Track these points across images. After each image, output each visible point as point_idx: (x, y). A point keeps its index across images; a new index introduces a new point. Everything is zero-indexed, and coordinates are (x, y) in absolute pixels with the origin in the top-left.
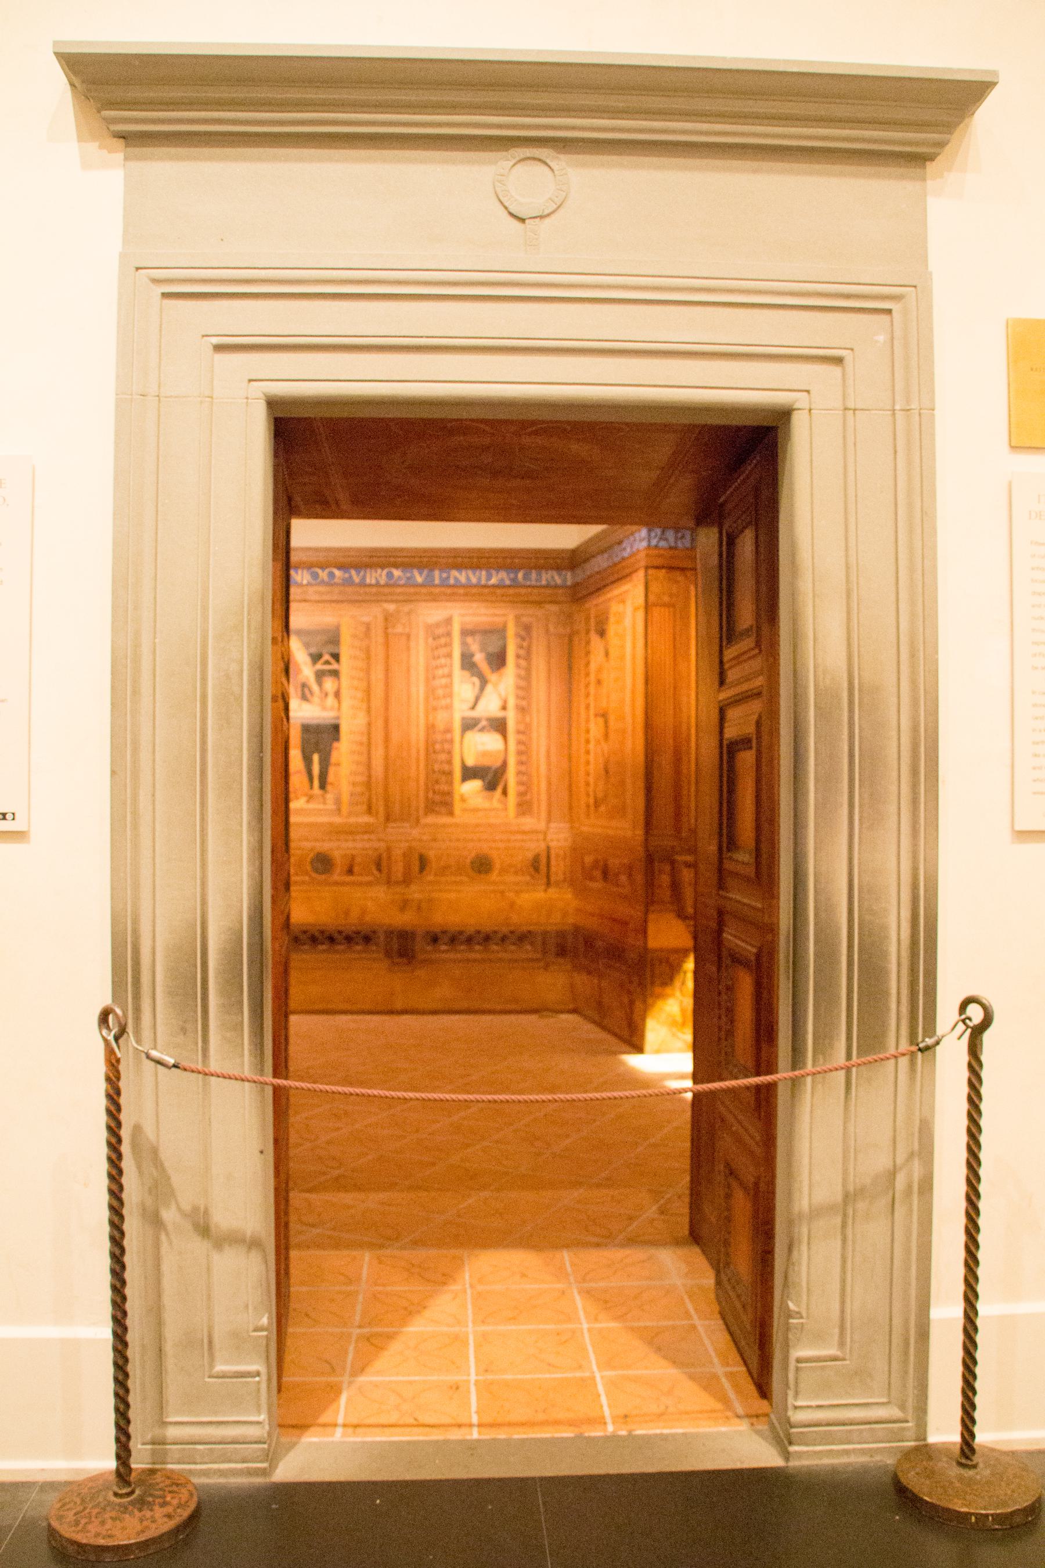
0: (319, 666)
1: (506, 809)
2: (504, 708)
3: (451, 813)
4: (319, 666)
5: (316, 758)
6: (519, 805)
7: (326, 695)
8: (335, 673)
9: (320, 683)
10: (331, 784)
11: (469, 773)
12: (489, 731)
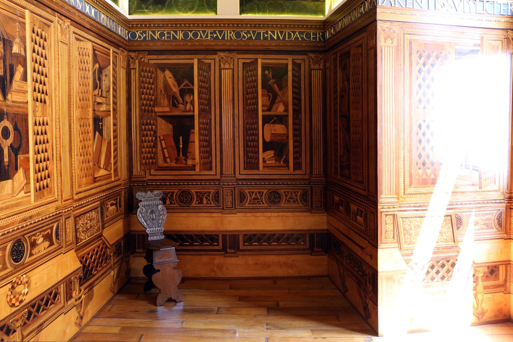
0: (182, 86)
1: (288, 167)
2: (286, 110)
3: (258, 168)
4: (182, 86)
5: (181, 138)
6: (294, 164)
7: (187, 103)
8: (192, 92)
9: (183, 97)
10: (190, 152)
11: (267, 147)
12: (278, 124)
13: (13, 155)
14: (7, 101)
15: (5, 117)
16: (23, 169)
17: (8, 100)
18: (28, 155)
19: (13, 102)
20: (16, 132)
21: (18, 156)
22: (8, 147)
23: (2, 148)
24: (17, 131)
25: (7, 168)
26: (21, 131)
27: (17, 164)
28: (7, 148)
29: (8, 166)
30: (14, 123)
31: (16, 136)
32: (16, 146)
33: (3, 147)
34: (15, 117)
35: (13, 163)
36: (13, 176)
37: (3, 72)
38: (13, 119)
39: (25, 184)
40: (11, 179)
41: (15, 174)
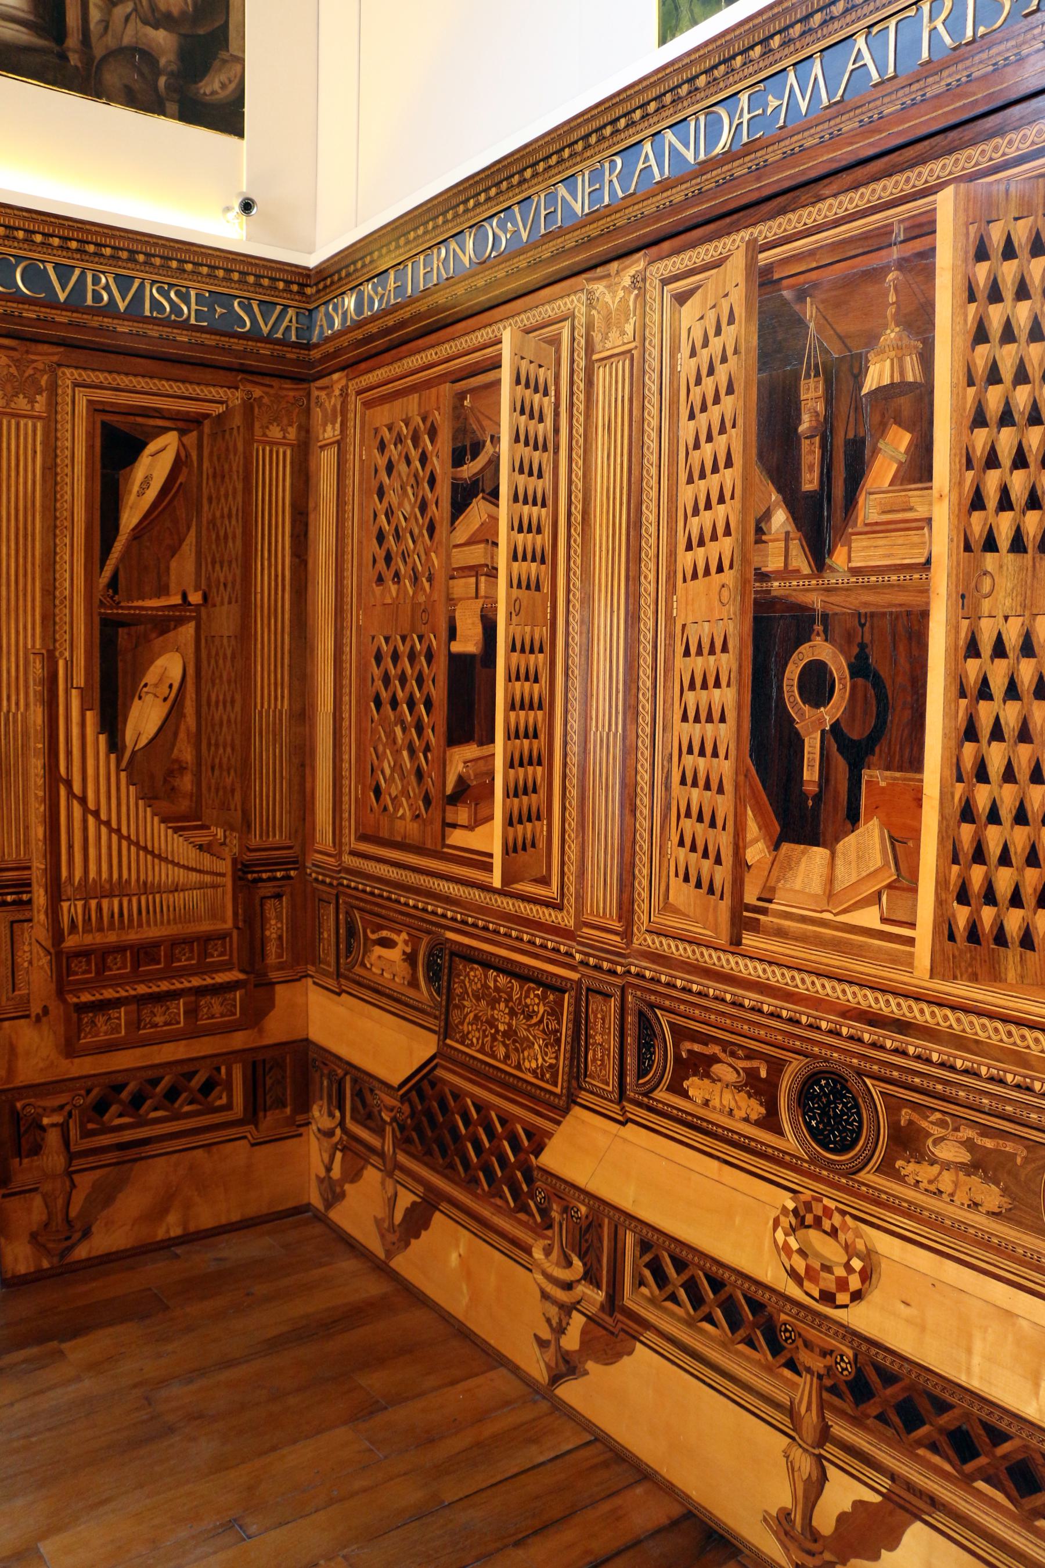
13: (841, 765)
14: (827, 574)
15: (819, 628)
16: (885, 824)
17: (833, 569)
18: (917, 776)
19: (855, 572)
20: (860, 681)
21: (866, 774)
22: (823, 732)
23: (797, 733)
24: (866, 677)
25: (810, 803)
26: (888, 683)
27: (858, 800)
28: (818, 735)
29: (818, 798)
30: (856, 650)
31: (860, 695)
32: (855, 734)
33: (802, 732)
34: (862, 625)
35: (836, 792)
36: (837, 840)
37: (816, 481)
38: (849, 637)
39: (890, 886)
40: (825, 846)
41: (846, 834)
